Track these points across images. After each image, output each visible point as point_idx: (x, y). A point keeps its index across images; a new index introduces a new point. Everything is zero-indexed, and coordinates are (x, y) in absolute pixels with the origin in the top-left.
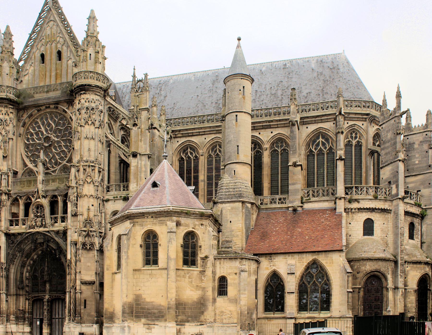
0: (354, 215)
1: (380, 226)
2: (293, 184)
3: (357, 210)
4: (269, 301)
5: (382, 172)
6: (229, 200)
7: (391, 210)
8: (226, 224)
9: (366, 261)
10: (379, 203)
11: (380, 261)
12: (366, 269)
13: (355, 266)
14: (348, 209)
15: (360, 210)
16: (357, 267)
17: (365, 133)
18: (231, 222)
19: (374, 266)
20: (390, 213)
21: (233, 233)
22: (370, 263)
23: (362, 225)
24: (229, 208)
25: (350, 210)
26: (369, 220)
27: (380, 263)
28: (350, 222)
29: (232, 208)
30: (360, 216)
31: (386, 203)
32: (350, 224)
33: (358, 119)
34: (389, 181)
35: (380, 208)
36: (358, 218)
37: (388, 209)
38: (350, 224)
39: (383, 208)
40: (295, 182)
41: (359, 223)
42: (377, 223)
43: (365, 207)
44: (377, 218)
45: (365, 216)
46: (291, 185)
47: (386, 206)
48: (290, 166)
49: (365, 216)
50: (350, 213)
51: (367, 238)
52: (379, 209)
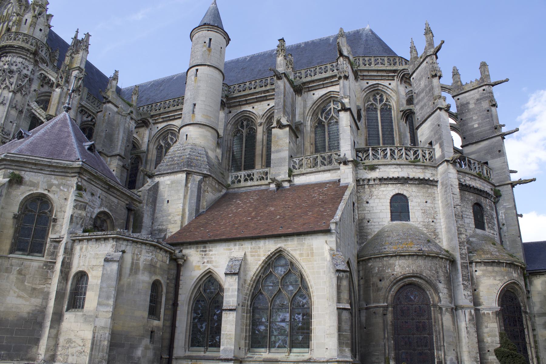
0: (373, 190)
1: (419, 206)
2: (278, 151)
3: (377, 182)
4: (199, 326)
5: (419, 132)
6: (169, 171)
7: (437, 182)
8: (161, 205)
9: (394, 258)
10: (415, 170)
11: (420, 258)
12: (395, 273)
13: (374, 268)
14: (363, 180)
15: (383, 181)
16: (378, 270)
17: (394, 94)
18: (168, 201)
19: (408, 266)
20: (437, 186)
21: (170, 218)
22: (400, 262)
23: (389, 204)
24: (169, 182)
25: (366, 182)
26: (399, 196)
27: (421, 262)
28: (368, 200)
29: (172, 183)
30: (383, 191)
31: (427, 171)
32: (367, 203)
33: (382, 78)
34: (429, 141)
35: (417, 177)
36: (381, 193)
37: (431, 179)
38: (367, 203)
39: (421, 178)
40: (280, 148)
41: (382, 201)
42: (415, 200)
43: (391, 176)
44: (414, 194)
45: (392, 190)
46: (274, 153)
47: (427, 175)
48: (274, 128)
49: (392, 190)
50: (366, 186)
51: (397, 225)
52: (413, 179)
